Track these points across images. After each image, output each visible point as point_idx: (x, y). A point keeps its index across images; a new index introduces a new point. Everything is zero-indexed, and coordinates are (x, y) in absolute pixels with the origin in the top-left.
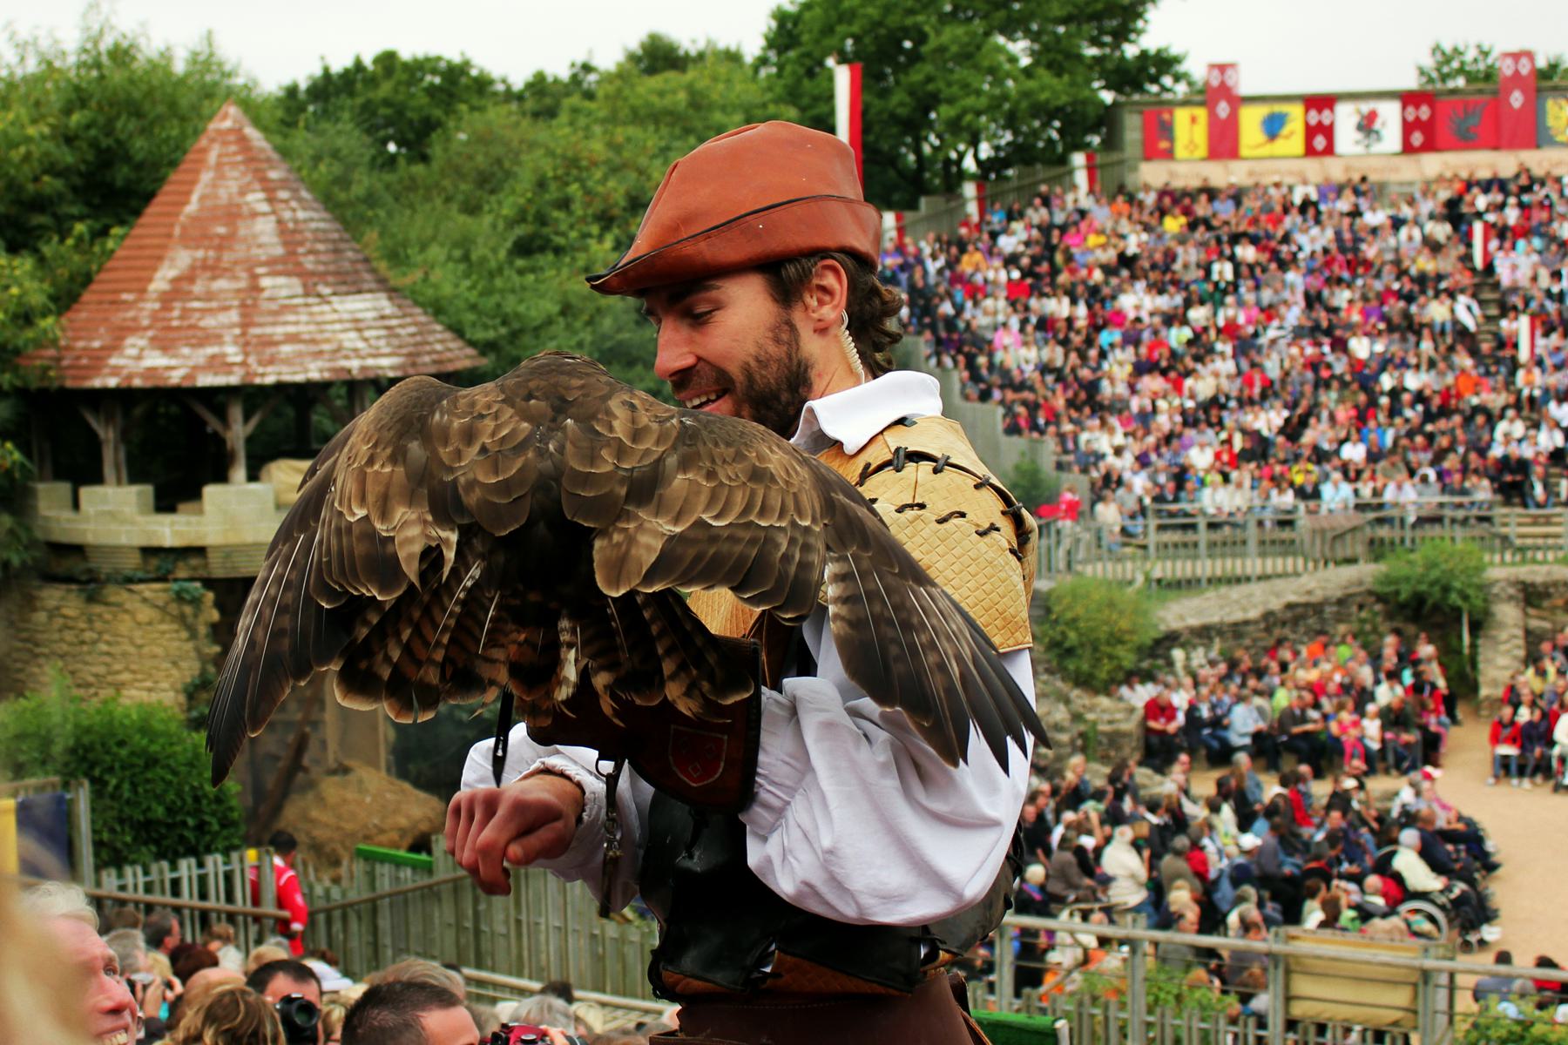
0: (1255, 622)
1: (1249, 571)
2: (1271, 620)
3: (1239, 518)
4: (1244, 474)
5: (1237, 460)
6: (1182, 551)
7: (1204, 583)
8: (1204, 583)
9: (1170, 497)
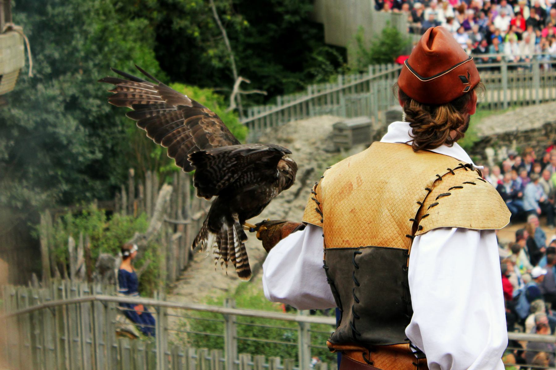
0: (539, 130)
1: (534, 97)
2: (549, 128)
3: (528, 63)
4: (530, 34)
5: (525, 25)
6: (491, 85)
7: (505, 105)
8: (505, 105)
9: (483, 50)
